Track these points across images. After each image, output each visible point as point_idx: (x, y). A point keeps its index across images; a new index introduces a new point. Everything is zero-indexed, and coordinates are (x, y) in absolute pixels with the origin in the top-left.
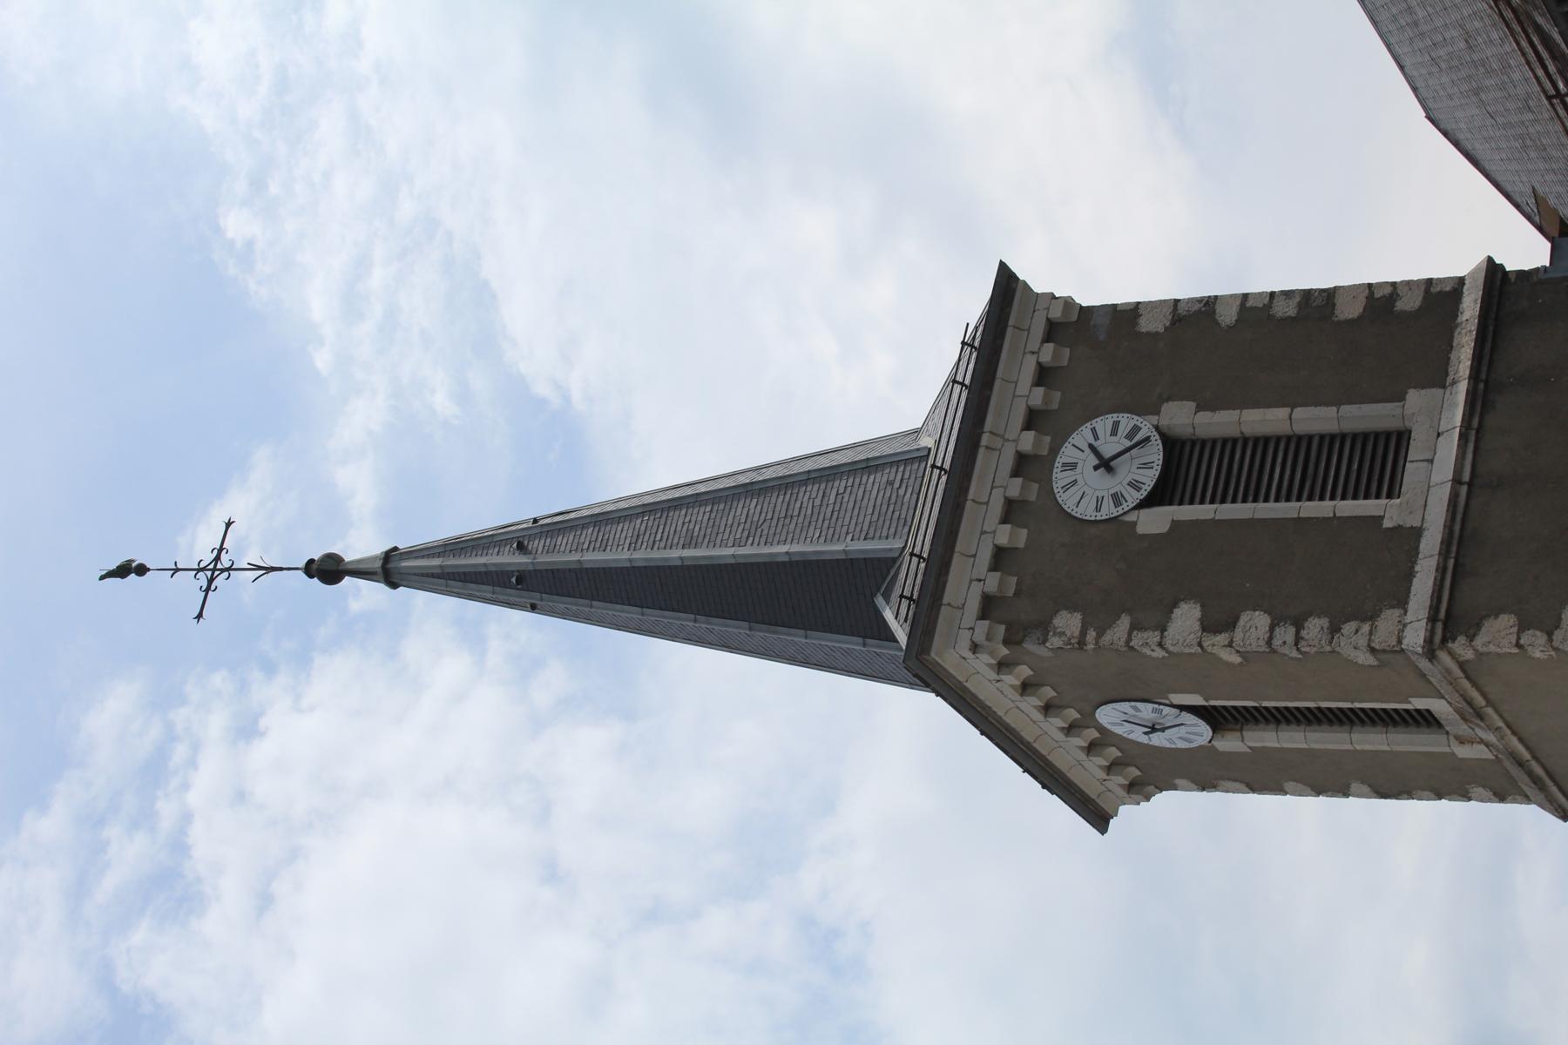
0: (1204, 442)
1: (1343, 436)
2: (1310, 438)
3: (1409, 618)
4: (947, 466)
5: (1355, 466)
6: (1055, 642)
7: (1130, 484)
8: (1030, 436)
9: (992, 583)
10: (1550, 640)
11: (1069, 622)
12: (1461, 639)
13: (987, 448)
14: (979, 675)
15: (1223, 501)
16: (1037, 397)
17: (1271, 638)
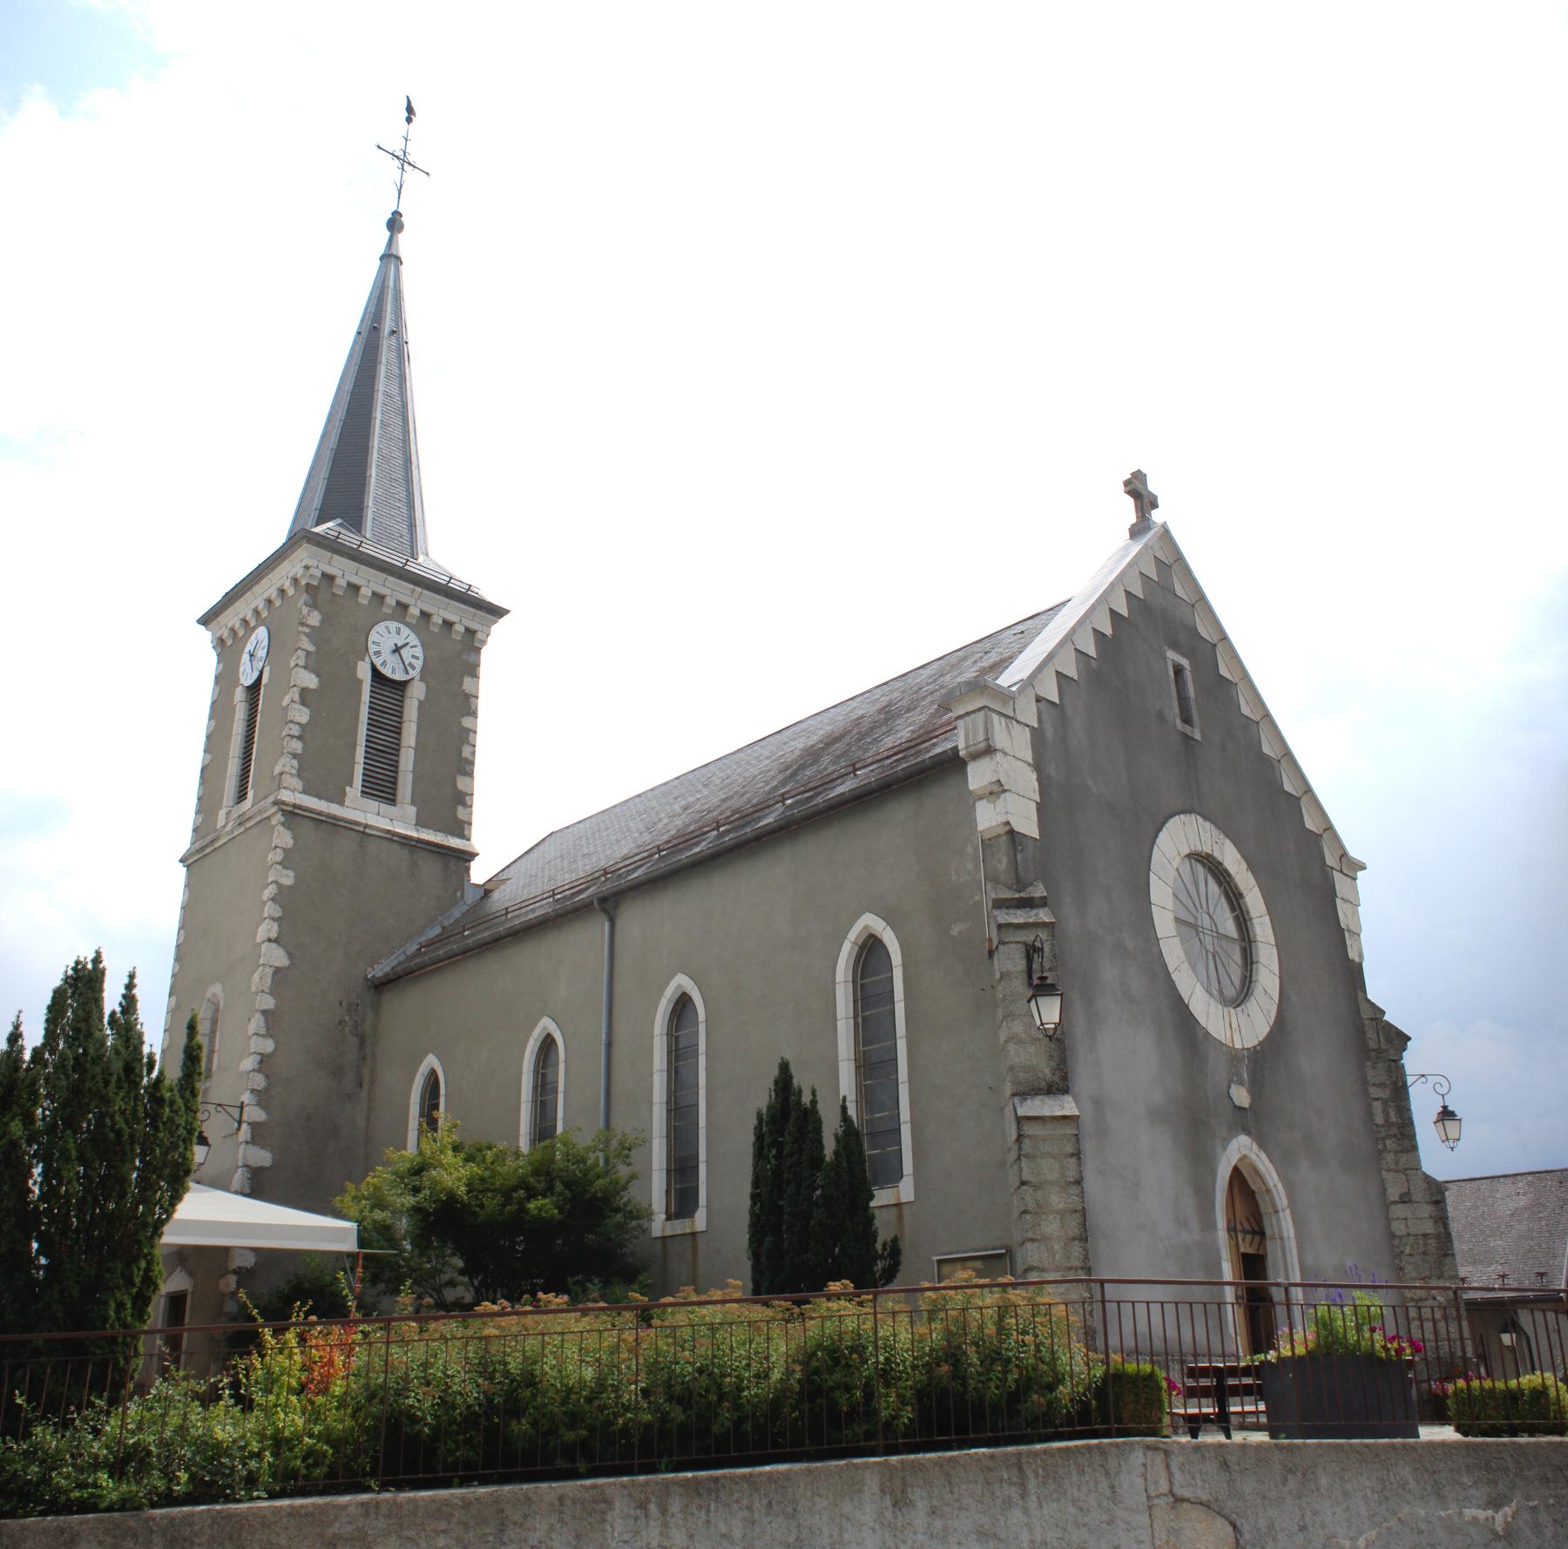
0: (402, 702)
1: (396, 772)
2: (398, 756)
3: (297, 794)
4: (407, 567)
5: (380, 776)
6: (305, 610)
8: (417, 613)
9: (341, 582)
10: (277, 863)
11: (315, 619)
12: (282, 819)
13: (414, 590)
14: (292, 567)
15: (370, 707)
16: (437, 620)
17: (294, 723)
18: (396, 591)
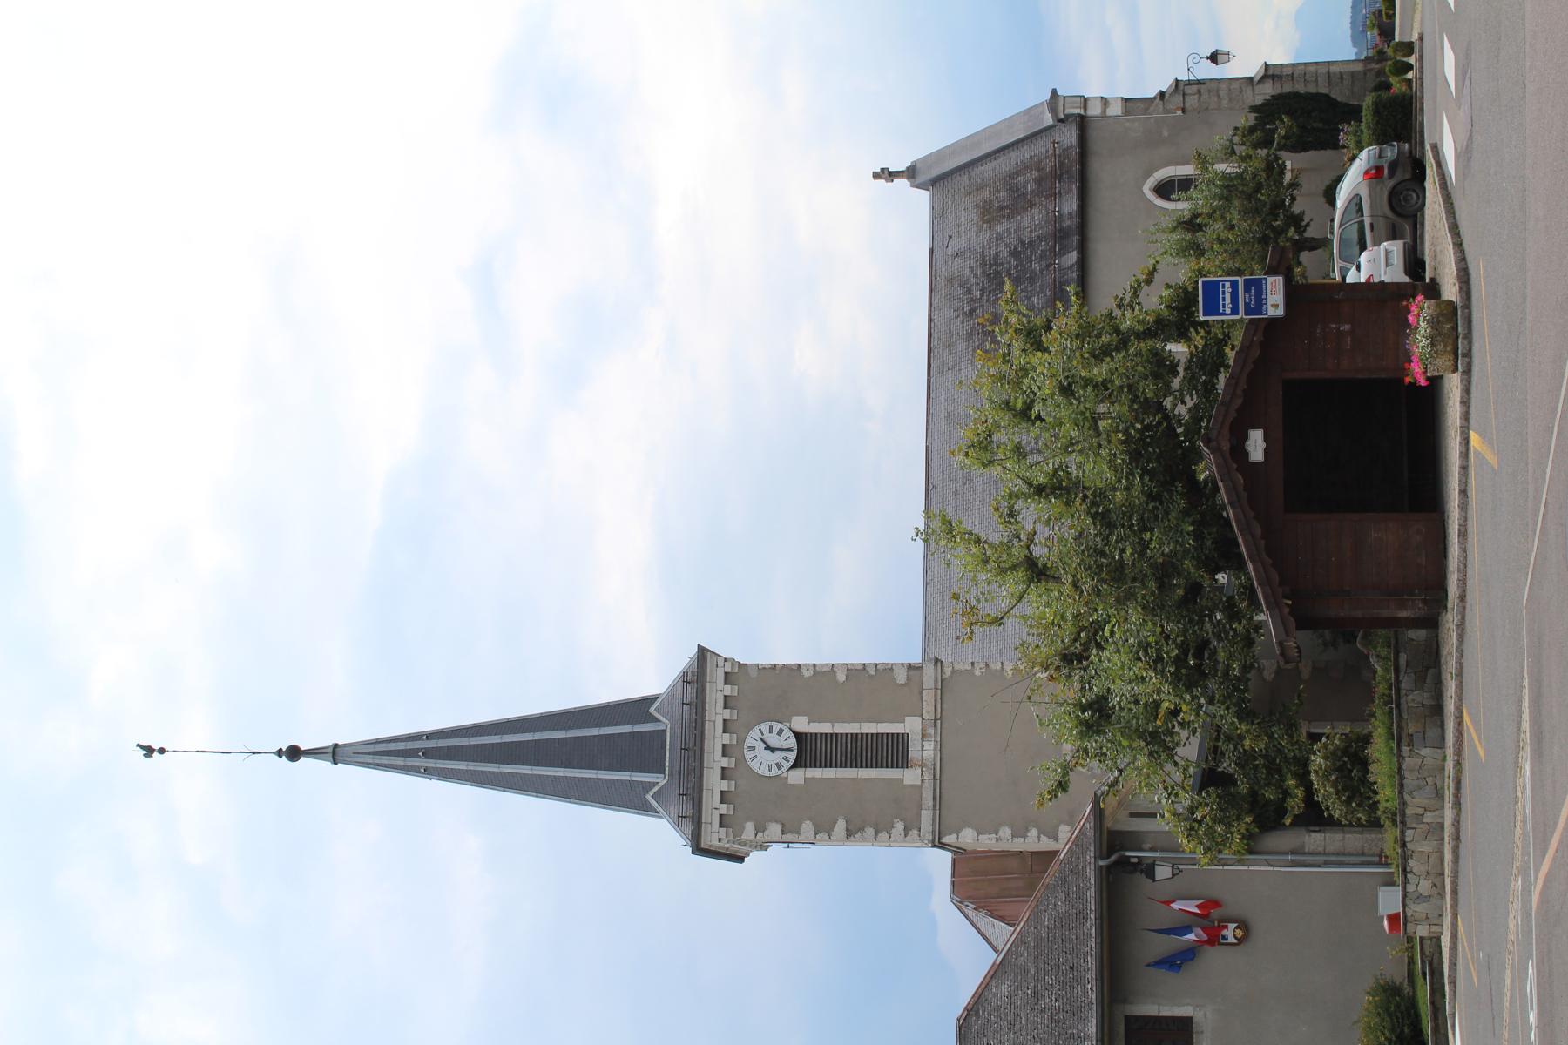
7: (783, 758)
18: (715, 761)
